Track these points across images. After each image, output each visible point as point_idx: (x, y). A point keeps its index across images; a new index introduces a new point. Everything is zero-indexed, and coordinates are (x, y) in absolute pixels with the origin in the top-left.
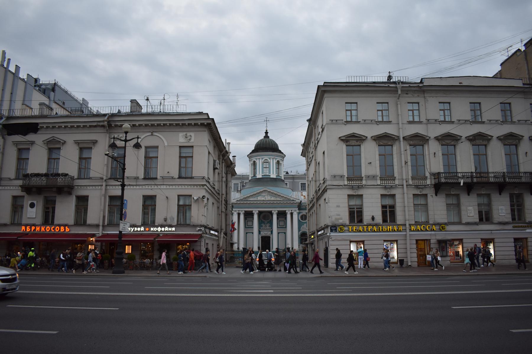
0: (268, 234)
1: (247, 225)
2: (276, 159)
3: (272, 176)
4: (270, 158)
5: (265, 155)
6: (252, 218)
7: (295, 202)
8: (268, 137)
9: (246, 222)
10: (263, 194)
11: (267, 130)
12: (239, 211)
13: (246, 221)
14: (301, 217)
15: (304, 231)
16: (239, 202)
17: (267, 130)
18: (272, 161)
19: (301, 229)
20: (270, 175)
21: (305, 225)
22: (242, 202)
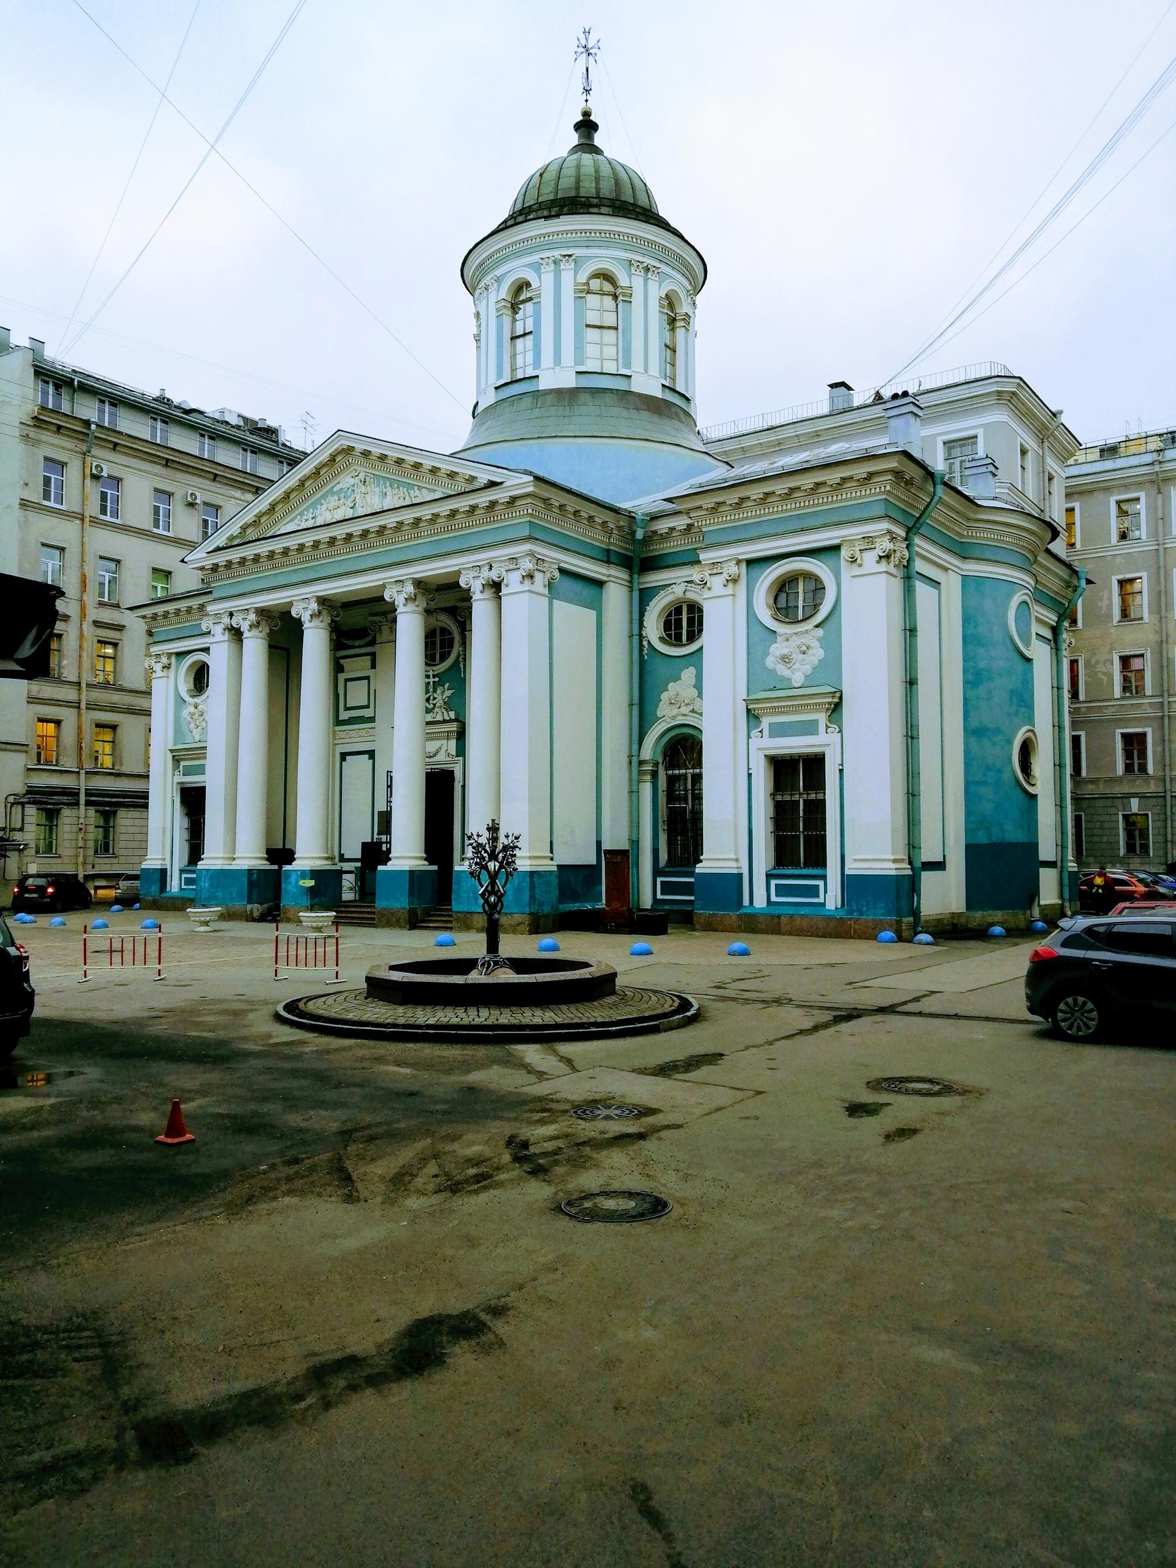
0: (441, 757)
1: (347, 709)
2: (578, 262)
3: (544, 384)
4: (537, 267)
5: (516, 255)
6: (367, 661)
7: (500, 495)
8: (597, 151)
9: (341, 691)
10: (346, 480)
11: (586, 114)
12: (231, 615)
13: (342, 677)
14: (667, 625)
15: (680, 720)
16: (221, 558)
17: (586, 114)
18: (548, 279)
19: (659, 714)
20: (538, 376)
21: (688, 674)
22: (234, 555)
